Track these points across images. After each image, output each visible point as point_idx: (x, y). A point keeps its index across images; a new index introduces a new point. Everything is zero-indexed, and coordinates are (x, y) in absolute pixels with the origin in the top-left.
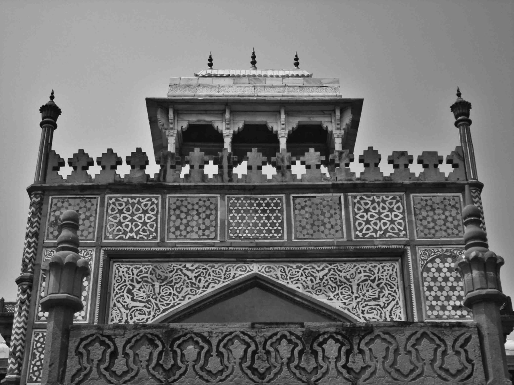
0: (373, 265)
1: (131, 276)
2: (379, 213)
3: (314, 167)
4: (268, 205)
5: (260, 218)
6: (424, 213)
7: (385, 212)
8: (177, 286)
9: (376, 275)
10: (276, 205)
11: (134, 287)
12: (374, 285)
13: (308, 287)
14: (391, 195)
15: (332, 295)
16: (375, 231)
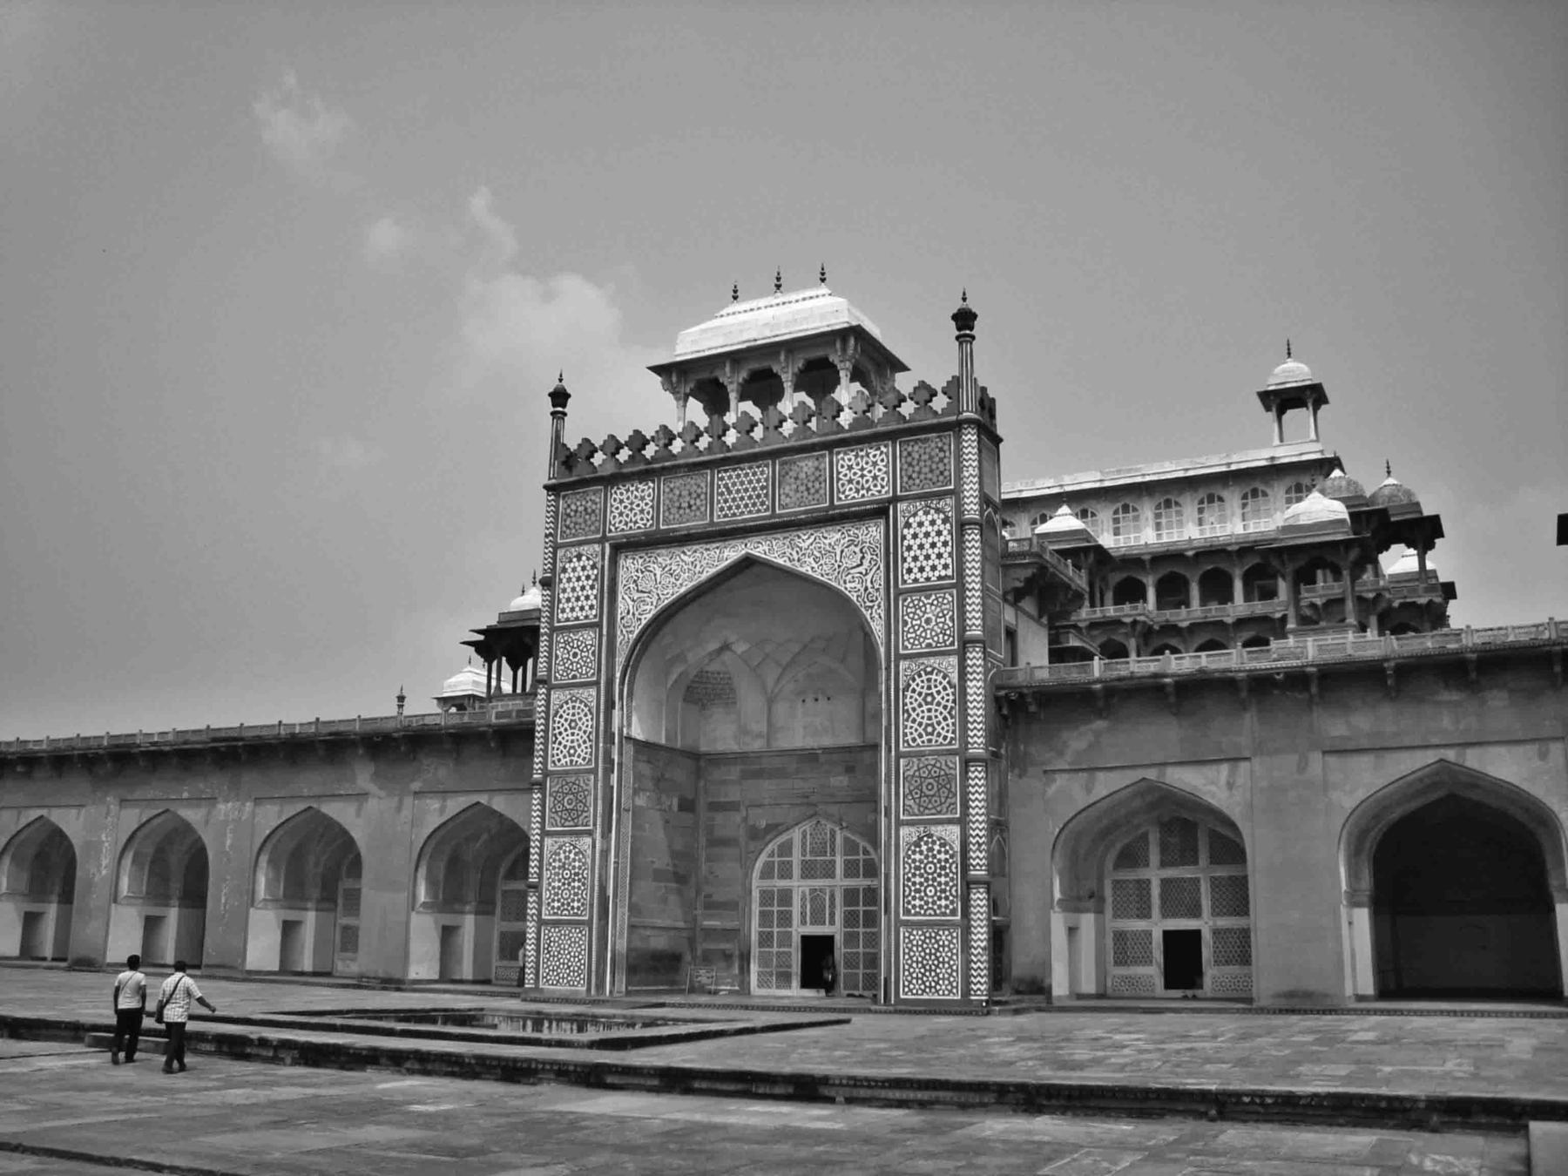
2: (862, 469)
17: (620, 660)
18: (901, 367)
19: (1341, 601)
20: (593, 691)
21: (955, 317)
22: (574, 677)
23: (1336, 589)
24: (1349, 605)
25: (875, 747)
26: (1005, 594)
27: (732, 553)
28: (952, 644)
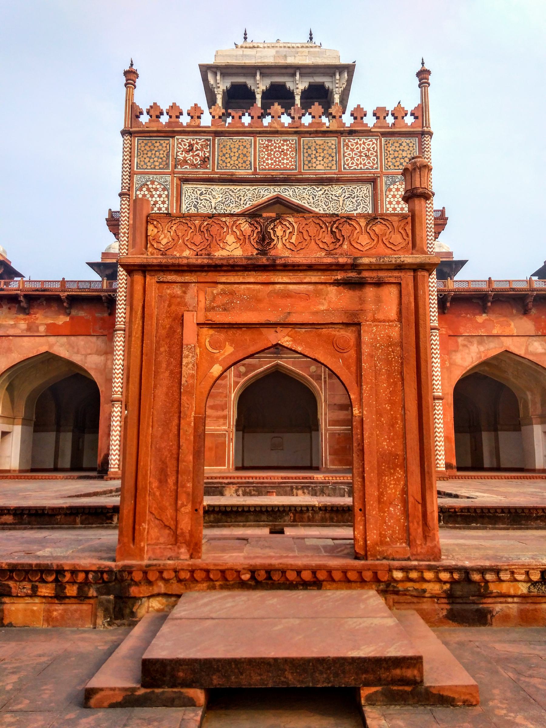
0: (354, 187)
1: (196, 195)
3: (317, 116)
8: (226, 203)
9: (356, 194)
11: (198, 203)
12: (354, 201)
13: (310, 202)
15: (326, 208)
27: (267, 193)
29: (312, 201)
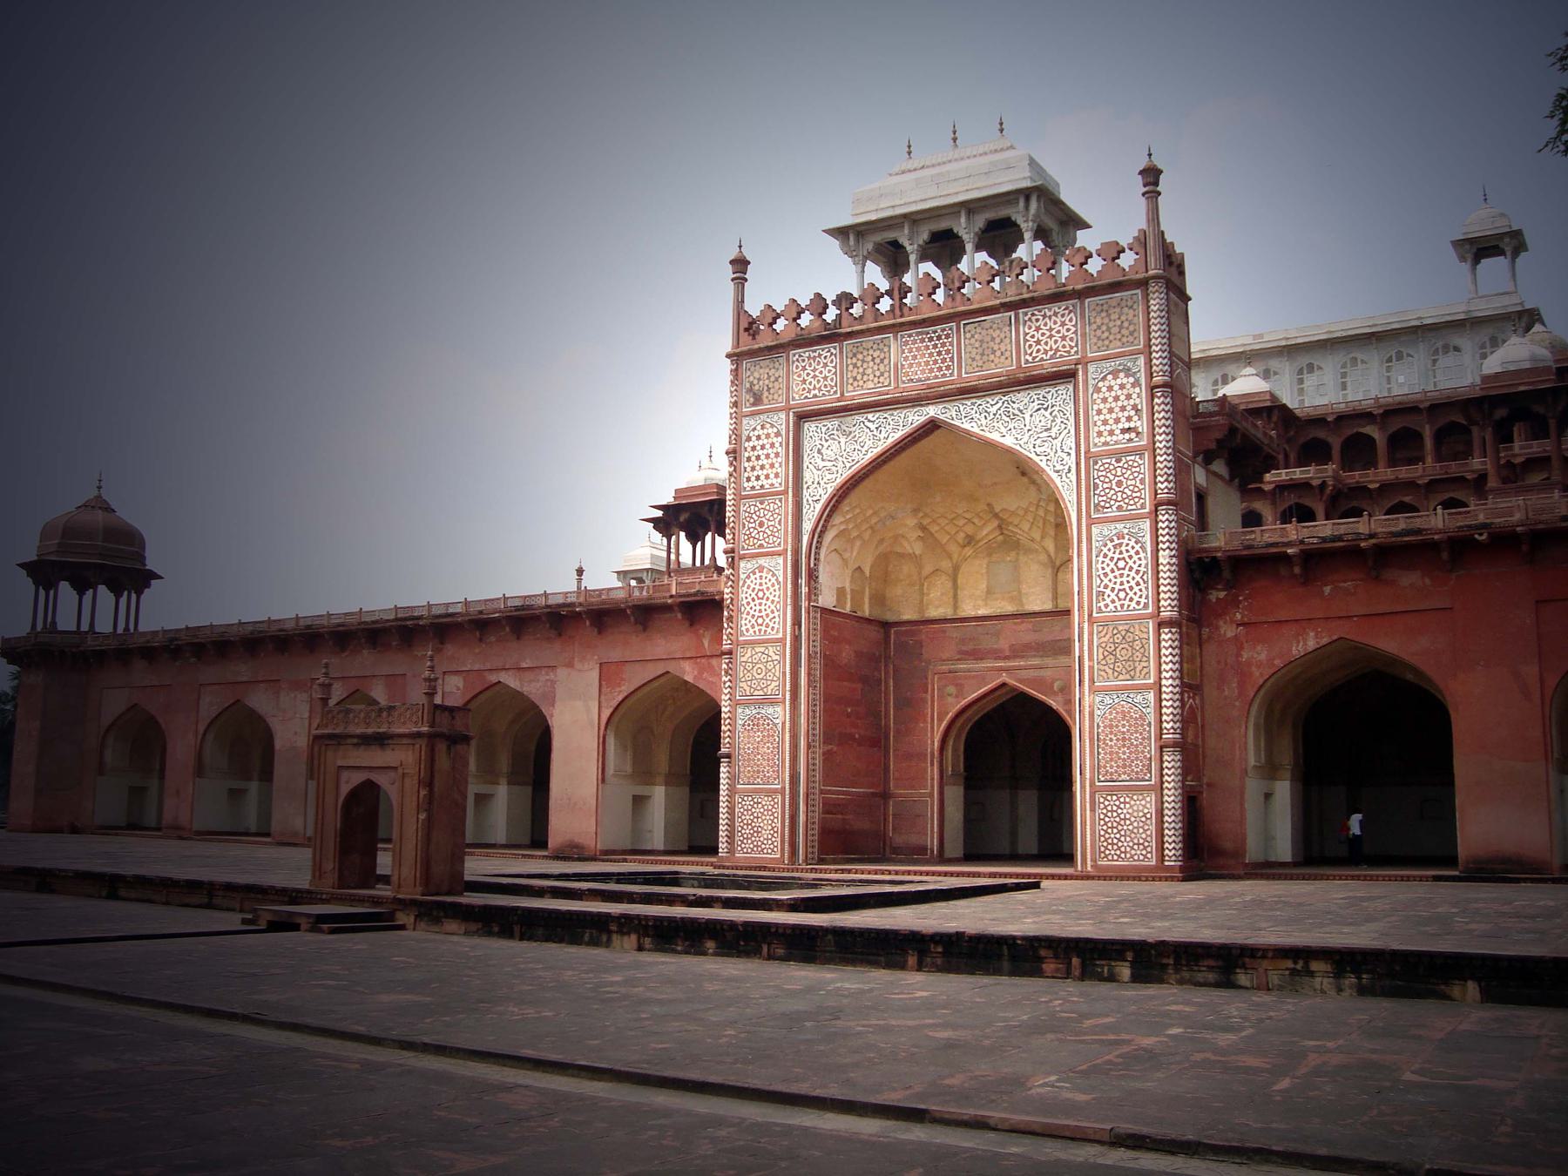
2: (1051, 330)
4: (939, 338)
5: (931, 355)
6: (1099, 321)
7: (1057, 327)
10: (947, 336)
12: (1047, 414)
14: (1063, 304)
16: (1046, 352)
17: (807, 526)
18: (1085, 225)
19: (1548, 459)
20: (780, 560)
21: (1141, 173)
22: (761, 546)
23: (1537, 448)
24: (1555, 463)
25: (1068, 612)
26: (1196, 455)
27: (915, 418)
28: (1143, 507)
29: (984, 422)
